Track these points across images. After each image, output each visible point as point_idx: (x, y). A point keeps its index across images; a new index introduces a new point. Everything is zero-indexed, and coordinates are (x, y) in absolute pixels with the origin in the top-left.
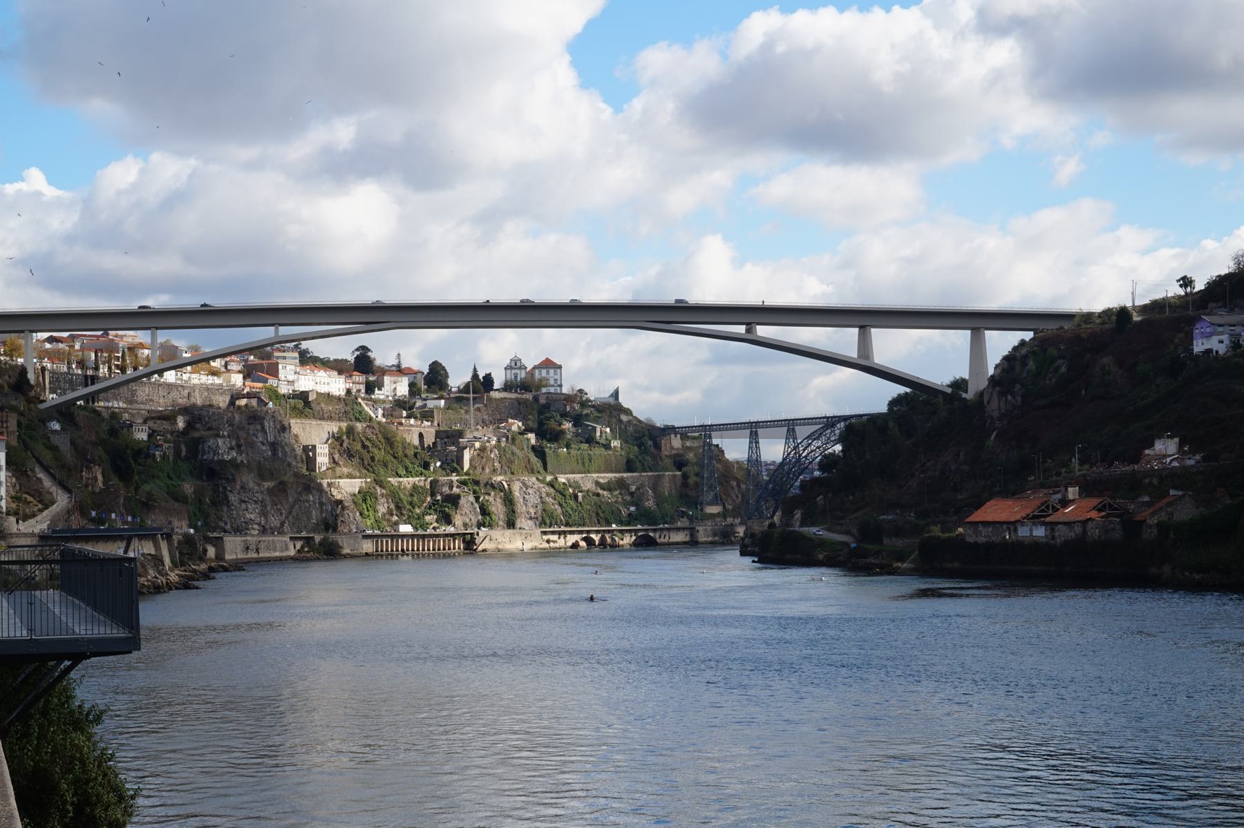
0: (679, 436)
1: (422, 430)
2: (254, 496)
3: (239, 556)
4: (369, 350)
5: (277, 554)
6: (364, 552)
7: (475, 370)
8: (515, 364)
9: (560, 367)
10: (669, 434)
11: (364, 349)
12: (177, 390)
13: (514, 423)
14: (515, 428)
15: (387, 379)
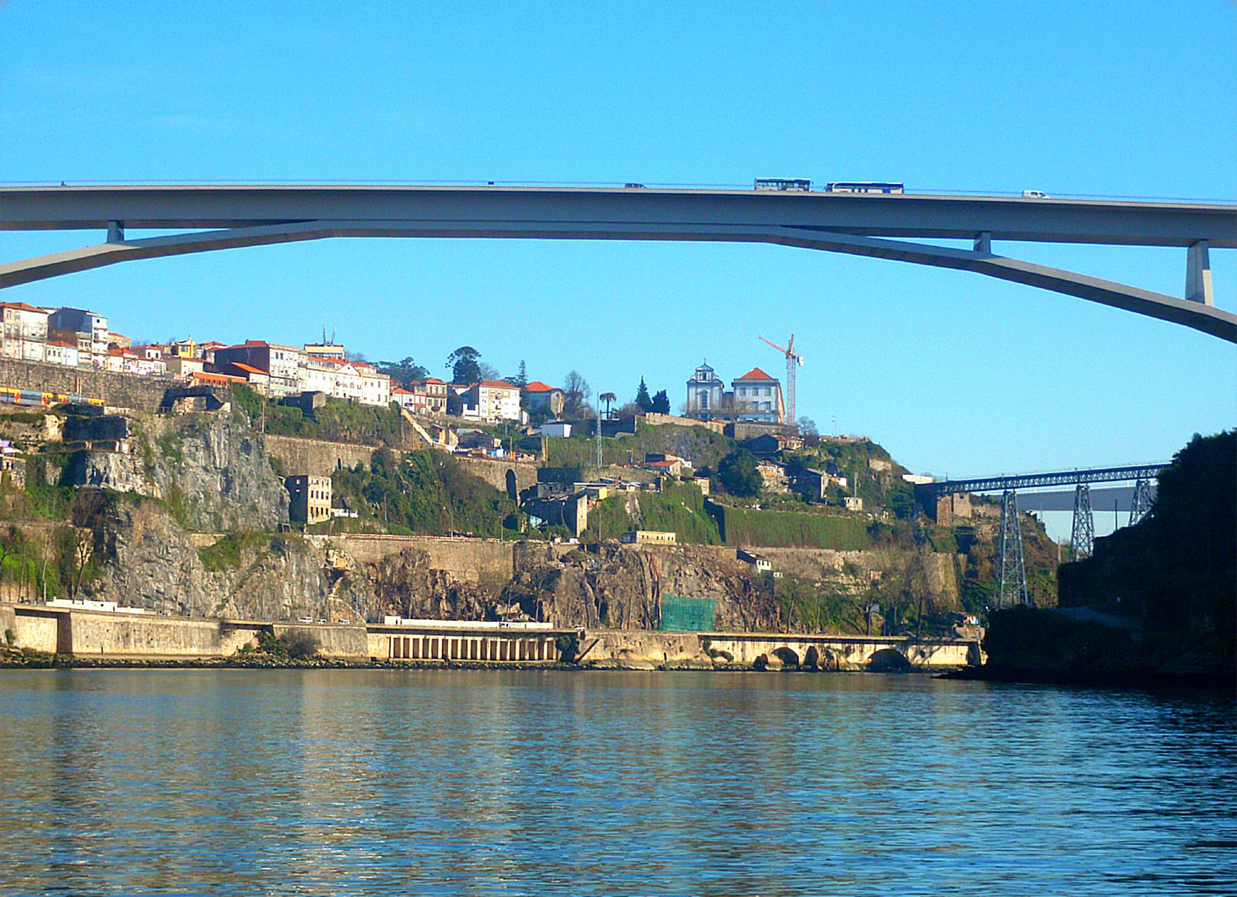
0: (967, 497)
1: (513, 466)
2: (168, 553)
3: (107, 650)
4: (477, 354)
5: (194, 651)
6: (370, 654)
7: (643, 387)
8: (704, 379)
9: (776, 383)
10: (951, 494)
11: (468, 350)
12: (64, 376)
13: (673, 462)
14: (675, 469)
15: (484, 392)
